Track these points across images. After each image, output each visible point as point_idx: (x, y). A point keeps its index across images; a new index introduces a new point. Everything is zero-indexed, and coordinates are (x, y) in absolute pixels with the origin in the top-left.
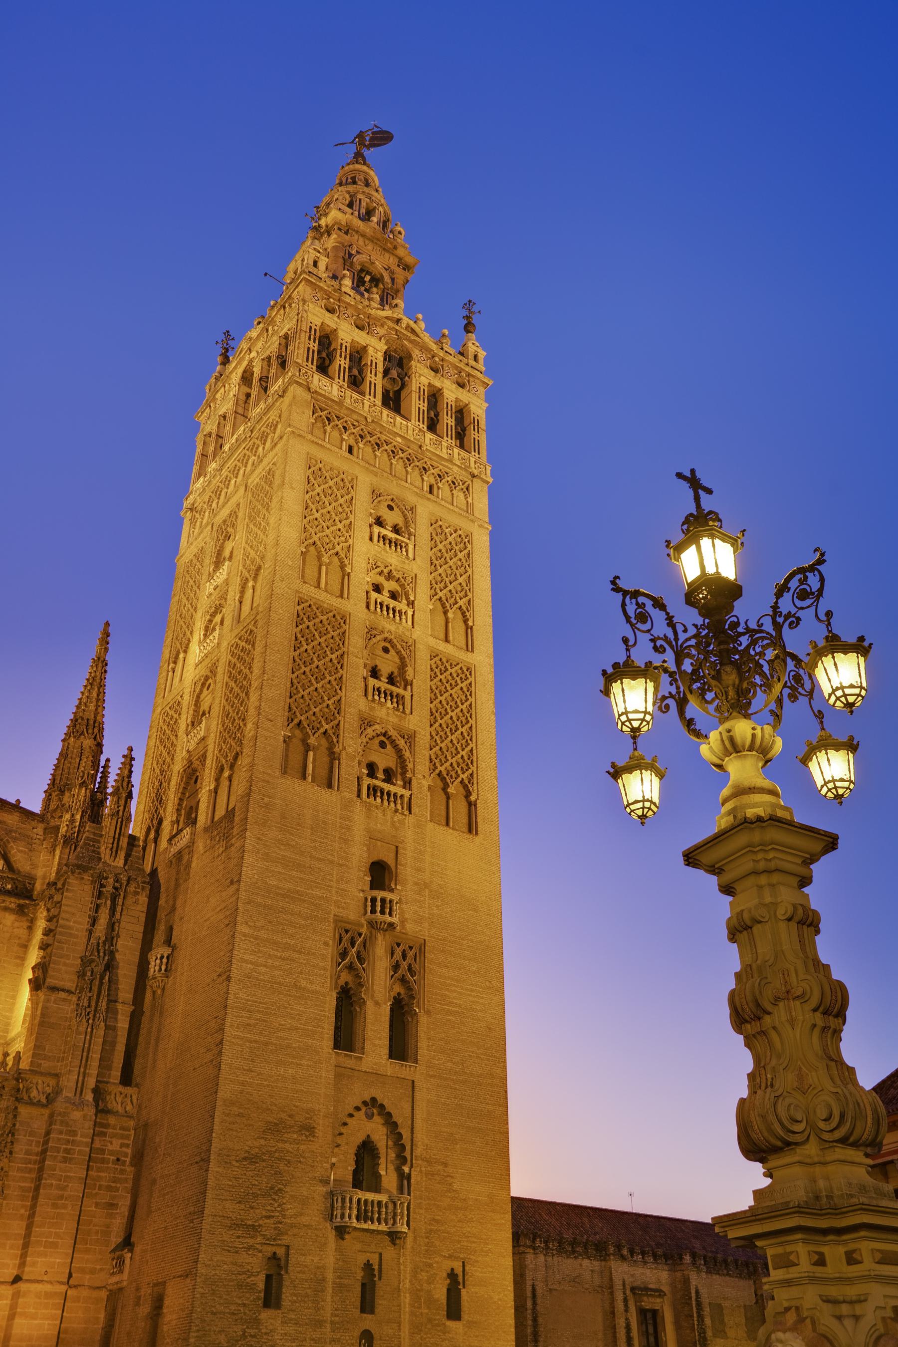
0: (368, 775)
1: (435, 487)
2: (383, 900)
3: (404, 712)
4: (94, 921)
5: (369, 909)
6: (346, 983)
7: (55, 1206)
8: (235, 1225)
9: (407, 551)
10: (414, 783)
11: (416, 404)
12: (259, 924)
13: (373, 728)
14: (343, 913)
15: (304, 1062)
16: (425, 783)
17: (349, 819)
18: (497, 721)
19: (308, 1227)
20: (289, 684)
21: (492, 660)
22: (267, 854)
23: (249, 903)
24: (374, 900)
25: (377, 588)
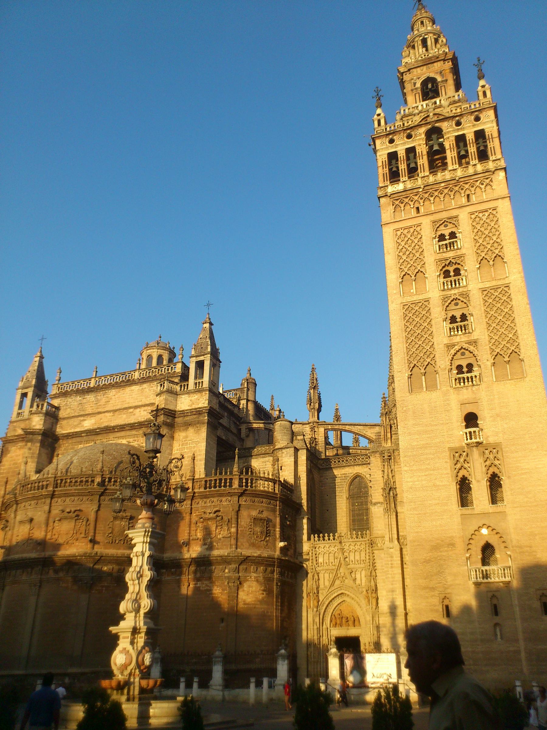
0: (457, 374)
1: (471, 195)
2: (470, 433)
3: (469, 333)
4: (383, 471)
5: (465, 439)
6: (464, 476)
7: (392, 584)
8: (425, 588)
9: (457, 245)
10: (482, 366)
11: (451, 155)
12: (411, 464)
13: (454, 349)
14: (452, 445)
15: (445, 517)
16: (489, 364)
17: (448, 400)
18: (531, 308)
19: (460, 585)
20: (405, 350)
21: (522, 274)
22: (409, 433)
23: (405, 457)
24: (466, 433)
25: (446, 274)
